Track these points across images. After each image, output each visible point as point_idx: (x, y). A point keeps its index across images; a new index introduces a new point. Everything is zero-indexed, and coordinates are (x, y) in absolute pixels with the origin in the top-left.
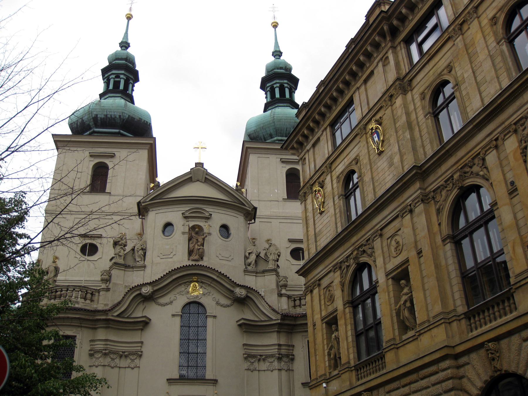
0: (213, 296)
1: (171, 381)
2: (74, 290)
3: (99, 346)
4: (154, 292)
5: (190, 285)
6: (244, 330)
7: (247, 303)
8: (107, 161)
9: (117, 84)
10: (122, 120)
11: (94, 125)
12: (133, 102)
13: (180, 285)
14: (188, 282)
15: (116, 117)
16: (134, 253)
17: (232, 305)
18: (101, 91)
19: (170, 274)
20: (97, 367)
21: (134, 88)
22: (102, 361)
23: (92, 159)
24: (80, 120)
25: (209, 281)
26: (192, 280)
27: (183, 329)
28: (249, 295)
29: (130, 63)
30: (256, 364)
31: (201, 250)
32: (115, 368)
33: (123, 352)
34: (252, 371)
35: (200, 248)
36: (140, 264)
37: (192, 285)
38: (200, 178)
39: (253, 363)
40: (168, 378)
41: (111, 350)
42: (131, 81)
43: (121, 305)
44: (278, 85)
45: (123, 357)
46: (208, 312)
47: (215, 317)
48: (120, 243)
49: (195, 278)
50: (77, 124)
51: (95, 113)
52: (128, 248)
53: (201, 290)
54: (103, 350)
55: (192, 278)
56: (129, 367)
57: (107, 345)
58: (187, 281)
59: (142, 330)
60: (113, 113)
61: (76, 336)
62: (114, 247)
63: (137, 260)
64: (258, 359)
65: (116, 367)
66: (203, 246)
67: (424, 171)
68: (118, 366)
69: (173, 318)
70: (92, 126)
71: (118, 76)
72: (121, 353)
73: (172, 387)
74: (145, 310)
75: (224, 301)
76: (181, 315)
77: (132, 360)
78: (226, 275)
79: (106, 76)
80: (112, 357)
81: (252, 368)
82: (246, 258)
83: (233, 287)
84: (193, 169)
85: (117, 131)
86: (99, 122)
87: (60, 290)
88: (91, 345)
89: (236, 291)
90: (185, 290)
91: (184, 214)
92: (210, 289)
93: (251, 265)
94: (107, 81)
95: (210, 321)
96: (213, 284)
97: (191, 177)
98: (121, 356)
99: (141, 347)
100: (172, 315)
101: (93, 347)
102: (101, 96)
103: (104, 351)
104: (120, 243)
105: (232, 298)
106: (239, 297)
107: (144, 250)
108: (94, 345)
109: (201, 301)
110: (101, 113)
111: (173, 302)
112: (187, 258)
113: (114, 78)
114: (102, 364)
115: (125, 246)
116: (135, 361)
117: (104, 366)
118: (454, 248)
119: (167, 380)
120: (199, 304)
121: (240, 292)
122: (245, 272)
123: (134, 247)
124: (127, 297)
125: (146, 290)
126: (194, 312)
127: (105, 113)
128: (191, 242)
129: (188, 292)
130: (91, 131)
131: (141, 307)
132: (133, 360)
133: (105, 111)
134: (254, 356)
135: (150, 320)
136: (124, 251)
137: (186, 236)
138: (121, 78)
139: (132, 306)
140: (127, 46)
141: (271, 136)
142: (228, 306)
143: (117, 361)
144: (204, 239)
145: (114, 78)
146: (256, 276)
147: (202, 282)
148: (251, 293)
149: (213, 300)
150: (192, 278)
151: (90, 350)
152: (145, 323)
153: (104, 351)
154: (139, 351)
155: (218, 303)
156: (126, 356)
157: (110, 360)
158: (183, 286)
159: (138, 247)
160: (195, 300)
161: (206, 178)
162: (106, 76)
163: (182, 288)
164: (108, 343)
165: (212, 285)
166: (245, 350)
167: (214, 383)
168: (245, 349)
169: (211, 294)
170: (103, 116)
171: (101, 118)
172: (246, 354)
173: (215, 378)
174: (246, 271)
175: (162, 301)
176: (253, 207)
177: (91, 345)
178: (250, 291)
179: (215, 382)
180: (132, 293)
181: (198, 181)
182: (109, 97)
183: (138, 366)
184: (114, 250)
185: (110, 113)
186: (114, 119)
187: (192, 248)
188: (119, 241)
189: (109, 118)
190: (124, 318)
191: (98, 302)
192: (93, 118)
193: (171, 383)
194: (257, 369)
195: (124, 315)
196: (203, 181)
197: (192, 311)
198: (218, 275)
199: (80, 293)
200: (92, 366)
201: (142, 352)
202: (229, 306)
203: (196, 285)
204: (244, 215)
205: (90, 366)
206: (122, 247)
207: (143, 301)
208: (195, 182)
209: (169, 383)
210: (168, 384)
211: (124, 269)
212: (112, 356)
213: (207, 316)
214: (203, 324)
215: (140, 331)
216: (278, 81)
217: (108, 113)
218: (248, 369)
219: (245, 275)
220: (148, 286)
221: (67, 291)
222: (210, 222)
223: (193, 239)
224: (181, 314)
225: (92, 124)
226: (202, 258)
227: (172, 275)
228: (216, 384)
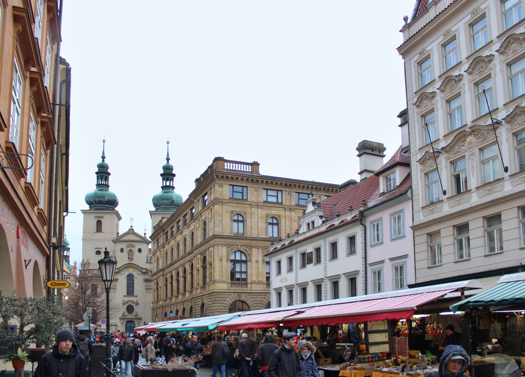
44: (166, 178)
47: (136, 278)
49: (130, 267)
75: (139, 273)
92: (136, 270)
95: (135, 279)
121: (144, 271)
137: (127, 253)
141: (161, 205)
142: (140, 274)
152: (117, 280)
155: (137, 274)
163: (127, 270)
174: (147, 262)
175: (121, 273)
179: (137, 296)
216: (166, 176)
222: (135, 248)
226: (132, 260)
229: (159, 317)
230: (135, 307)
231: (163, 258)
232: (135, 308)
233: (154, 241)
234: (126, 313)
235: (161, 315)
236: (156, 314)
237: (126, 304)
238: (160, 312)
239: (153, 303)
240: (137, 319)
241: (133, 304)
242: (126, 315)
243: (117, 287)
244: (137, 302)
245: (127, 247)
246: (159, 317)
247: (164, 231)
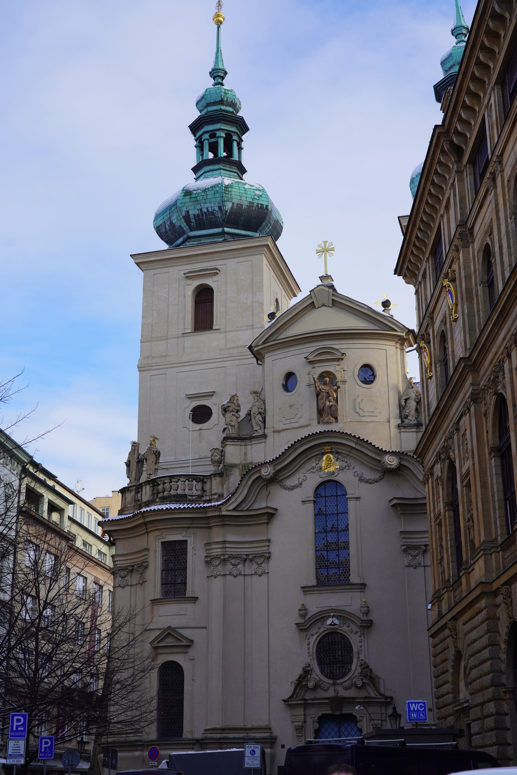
0: (354, 470)
1: (306, 589)
2: (179, 480)
3: (216, 551)
4: (277, 473)
5: (322, 457)
6: (400, 512)
7: (402, 473)
8: (209, 281)
9: (214, 148)
10: (224, 212)
11: (187, 227)
12: (242, 170)
14: (319, 454)
15: (214, 210)
16: (250, 420)
17: (381, 479)
18: (194, 163)
19: (293, 447)
20: (216, 577)
21: (243, 145)
22: (220, 570)
23: (189, 282)
24: (168, 223)
25: (347, 451)
26: (323, 451)
27: (318, 519)
28: (404, 463)
29: (230, 106)
30: (420, 558)
31: (333, 408)
32: (238, 577)
33: (247, 555)
34: (415, 568)
35: (332, 405)
36: (259, 434)
37: (324, 458)
38: (326, 302)
39: (415, 556)
40: (302, 586)
41: (232, 555)
42: (235, 137)
43: (237, 495)
45: (247, 563)
46: (349, 491)
47: (358, 498)
48: (231, 409)
49: (327, 448)
50: (165, 227)
51: (184, 209)
52: (243, 414)
53: (337, 463)
54: (221, 555)
55: (324, 449)
56: (256, 574)
57: (226, 548)
58: (318, 453)
59: (268, 523)
61: (186, 541)
62: (223, 415)
63: (255, 429)
64: (422, 550)
65: (240, 574)
66: (337, 401)
67: (474, 362)
68: (242, 573)
69: (304, 505)
70: (185, 229)
71: (213, 134)
72: (245, 557)
73: (308, 596)
74: (269, 498)
75: (369, 475)
76: (314, 501)
77: (259, 564)
78: (367, 441)
79: (198, 135)
80: (233, 562)
81: (414, 563)
82: (401, 408)
83: (380, 455)
84: (313, 290)
85: (219, 230)
86: (193, 220)
87: (163, 482)
88: (207, 550)
89: (384, 460)
90: (317, 466)
91: (308, 359)
92: (349, 460)
93: (409, 418)
94: (199, 145)
97: (313, 302)
98: (245, 561)
99: (268, 546)
100: (303, 501)
101: (210, 552)
102: (195, 170)
103: (222, 557)
104: (231, 409)
105: (380, 469)
106: (389, 469)
107: (263, 415)
108: (210, 549)
109: (338, 478)
111: (303, 483)
112: (316, 421)
113: (208, 140)
114: (222, 573)
115: (238, 411)
116: (263, 565)
117: (225, 575)
118: (499, 463)
119: (302, 588)
120: (337, 484)
122: (400, 429)
123: (250, 411)
124: (245, 482)
125: (267, 472)
126: (331, 494)
127: (199, 207)
128: (320, 397)
129: (321, 468)
130: (185, 236)
131: (264, 492)
132: (260, 565)
134: (416, 547)
135: (276, 510)
136: (237, 418)
138: (218, 137)
139: (252, 495)
140: (222, 75)
142: (376, 481)
143: (240, 567)
144: (336, 391)
145: (208, 140)
146: (416, 432)
147: (337, 453)
148: (406, 460)
149: (354, 476)
150: (324, 449)
151: (206, 557)
154: (266, 553)
155: (361, 480)
156: (251, 560)
157: (232, 567)
158: (313, 460)
159: (255, 410)
160: (330, 478)
161: (333, 300)
162: (198, 135)
163: (312, 463)
164: (227, 545)
165: (351, 454)
166: (404, 540)
167: (361, 589)
168: (403, 538)
169: (351, 468)
170: (197, 212)
171: (194, 215)
172: (404, 545)
173: (362, 582)
176: (407, 331)
177: (207, 550)
178: (405, 458)
179: (363, 586)
180: (250, 477)
181: (323, 305)
182: (205, 172)
183: (266, 571)
184: (224, 418)
186: (213, 213)
188: (229, 406)
189: (205, 213)
190: (242, 511)
191: (211, 492)
192: (184, 217)
193: (306, 591)
194: (422, 564)
195: (244, 506)
196: (331, 306)
197: (328, 494)
199: (187, 482)
200: (211, 576)
201: (269, 553)
202: (377, 481)
203: (330, 458)
204: (396, 343)
205: (208, 577)
206: (234, 413)
207: (267, 485)
208: (319, 307)
209: (304, 591)
210: (302, 594)
211: (239, 443)
212: (233, 561)
213: (347, 498)
214: (344, 510)
218: (409, 566)
219: (400, 432)
221: (171, 482)
222: (344, 364)
223: (322, 393)
224: (314, 499)
225: (184, 225)
226: (336, 418)
227: (296, 449)
228: (364, 589)
229: (474, 673)
230: (355, 640)
231: (470, 299)
232: (355, 650)
233: (420, 278)
234: (317, 674)
235: (486, 653)
236: (459, 656)
237: (314, 630)
238: (474, 635)
239: (437, 598)
240: (367, 702)
241: (345, 629)
242: (316, 687)
243: (274, 549)
244: (367, 613)
245: (310, 362)
246: (474, 673)
247: (458, 151)
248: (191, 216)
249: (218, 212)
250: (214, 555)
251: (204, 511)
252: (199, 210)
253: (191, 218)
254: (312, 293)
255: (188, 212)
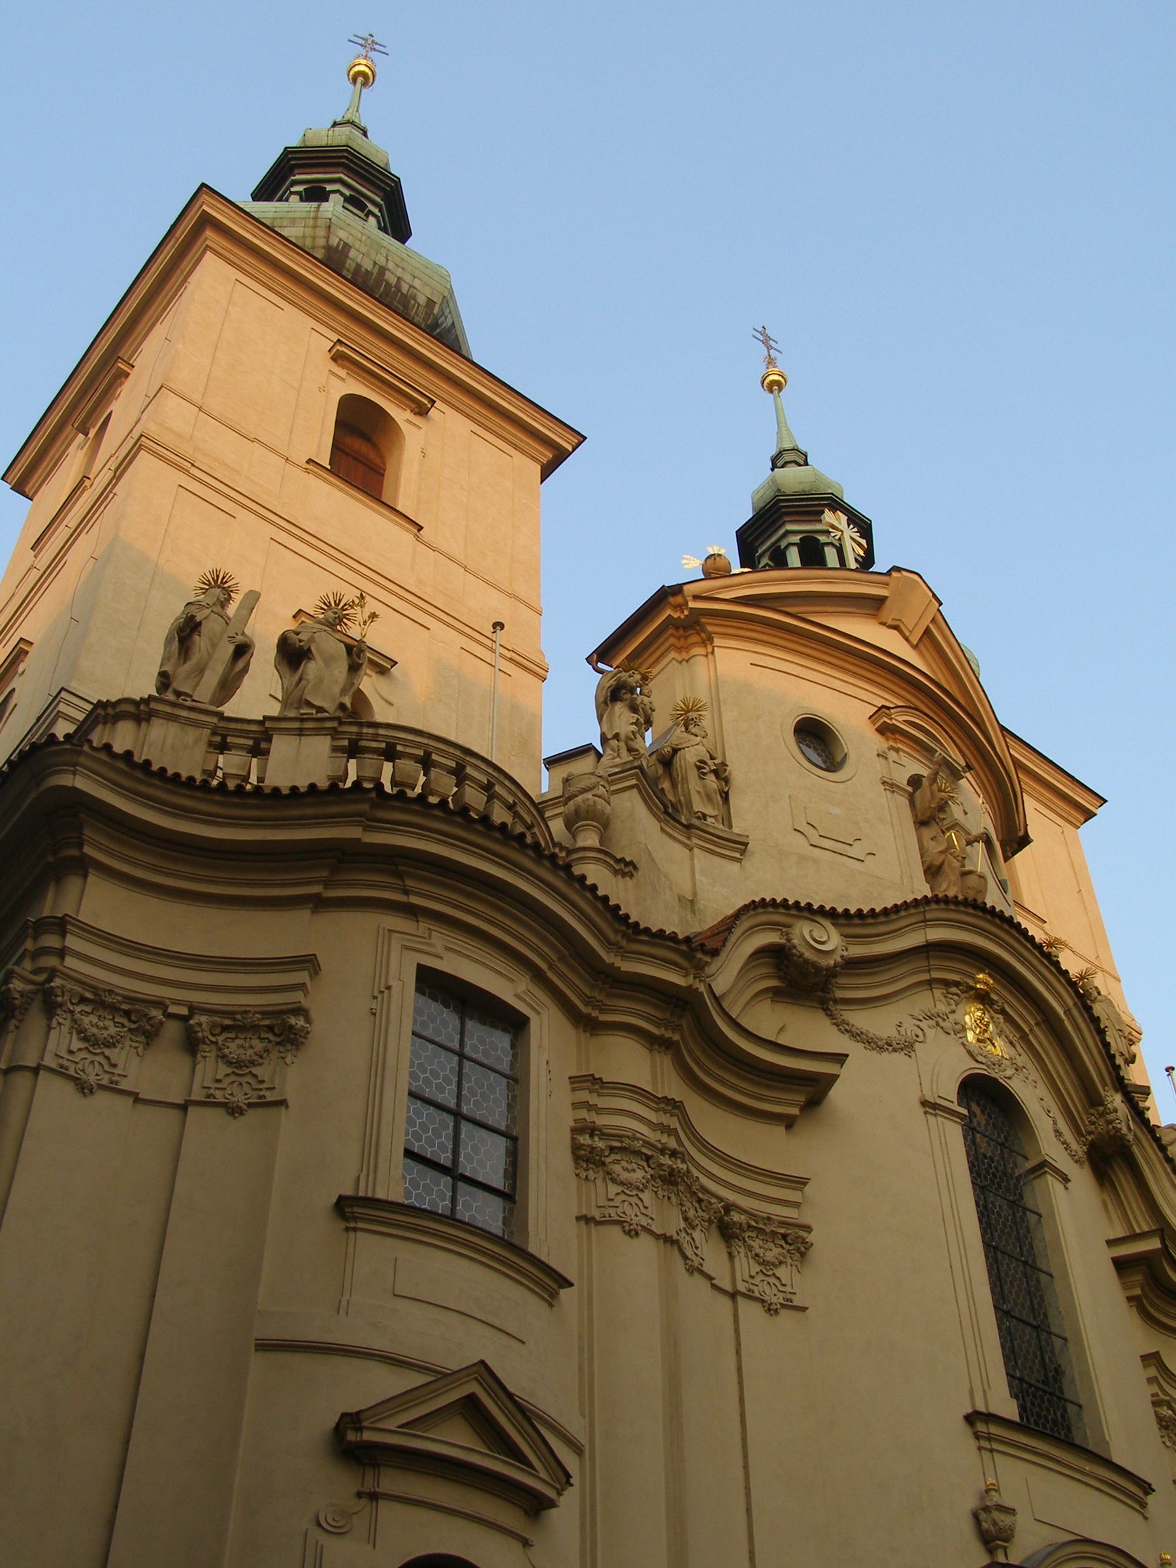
13: (930, 983)
14: (957, 984)
15: (414, 298)
20: (632, 1233)
25: (1026, 1022)
51: (342, 234)
54: (663, 1151)
60: (408, 278)
77: (764, 1263)
83: (1104, 1084)
91: (889, 717)
96: (1036, 1037)
97: (882, 600)
100: (924, 1103)
108: (600, 1111)
110: (364, 249)
127: (381, 261)
133: (384, 252)
153: (666, 1160)
170: (367, 265)
171: (359, 266)
181: (896, 628)
185: (399, 272)
187: (941, 860)
189: (388, 284)
198: (1070, 1003)
215: (780, 1130)
217: (391, 265)
220: (827, 924)
248: (349, 261)
249: (421, 309)
250: (634, 1138)
251: (624, 943)
252: (378, 266)
253: (347, 265)
254: (894, 574)
255: (347, 247)
